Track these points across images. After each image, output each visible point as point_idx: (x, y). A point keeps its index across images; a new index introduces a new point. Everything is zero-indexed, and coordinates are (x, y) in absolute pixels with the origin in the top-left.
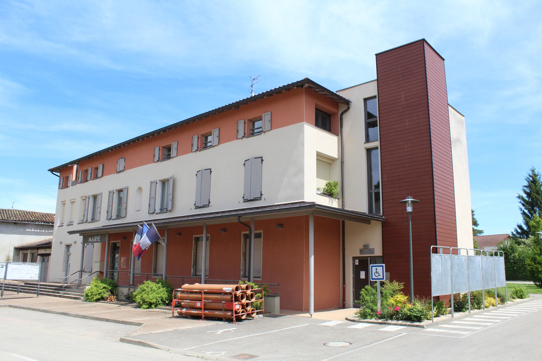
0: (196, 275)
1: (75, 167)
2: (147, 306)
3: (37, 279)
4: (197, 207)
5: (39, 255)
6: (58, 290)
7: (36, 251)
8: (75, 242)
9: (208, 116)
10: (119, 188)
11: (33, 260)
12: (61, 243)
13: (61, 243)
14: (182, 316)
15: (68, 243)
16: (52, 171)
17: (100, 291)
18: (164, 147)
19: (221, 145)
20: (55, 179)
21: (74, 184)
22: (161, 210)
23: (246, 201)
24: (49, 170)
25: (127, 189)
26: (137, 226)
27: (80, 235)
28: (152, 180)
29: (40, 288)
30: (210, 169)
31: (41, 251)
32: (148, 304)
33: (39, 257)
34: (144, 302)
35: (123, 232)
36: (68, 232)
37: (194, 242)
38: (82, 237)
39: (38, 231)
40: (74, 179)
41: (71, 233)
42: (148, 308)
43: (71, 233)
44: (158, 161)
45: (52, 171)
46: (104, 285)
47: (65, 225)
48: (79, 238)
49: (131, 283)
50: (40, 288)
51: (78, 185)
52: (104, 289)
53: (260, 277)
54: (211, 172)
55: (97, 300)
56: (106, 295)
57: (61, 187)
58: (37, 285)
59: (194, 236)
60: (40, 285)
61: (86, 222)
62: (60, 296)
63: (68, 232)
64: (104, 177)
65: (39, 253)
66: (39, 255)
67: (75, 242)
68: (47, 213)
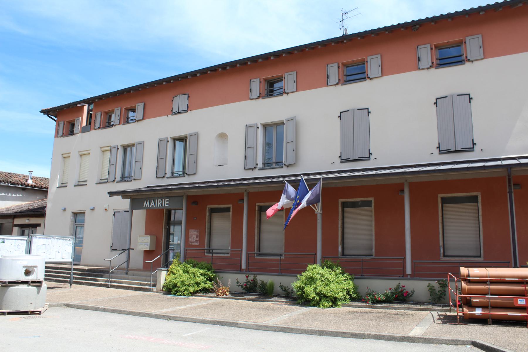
0: (343, 255)
1: (86, 108)
2: (331, 304)
3: (69, 259)
4: (343, 161)
5: (16, 225)
6: (92, 275)
7: (10, 220)
8: (93, 209)
9: (313, 48)
10: (125, 143)
11: (23, 234)
12: (65, 210)
13: (65, 210)
14: (448, 320)
15: (78, 209)
16: (47, 112)
17: (198, 279)
18: (265, 80)
19: (385, 78)
20: (50, 125)
21: (84, 130)
22: (173, 173)
23: (442, 153)
24: (40, 112)
25: (196, 135)
26: (282, 182)
27: (124, 198)
28: (249, 123)
29: (74, 274)
30: (368, 109)
31: (18, 221)
32: (331, 301)
33: (16, 229)
34: (322, 296)
35: (221, 192)
36: (109, 193)
37: (207, 214)
38: (128, 201)
39: (3, 194)
40: (84, 124)
41: (111, 194)
42: (332, 306)
43: (111, 194)
44: (99, 128)
45: (47, 112)
46: (202, 271)
47: (71, 185)
48: (127, 203)
49: (244, 266)
50: (74, 274)
51: (92, 132)
52: (202, 278)
53: (480, 257)
54: (369, 112)
55: (195, 293)
56: (209, 285)
57: (60, 133)
58: (70, 269)
59: (341, 201)
60: (74, 269)
61: (114, 181)
62: (101, 285)
63: (109, 193)
64: (144, 121)
65: (15, 223)
66: (16, 225)
67: (93, 209)
68: (9, 172)
